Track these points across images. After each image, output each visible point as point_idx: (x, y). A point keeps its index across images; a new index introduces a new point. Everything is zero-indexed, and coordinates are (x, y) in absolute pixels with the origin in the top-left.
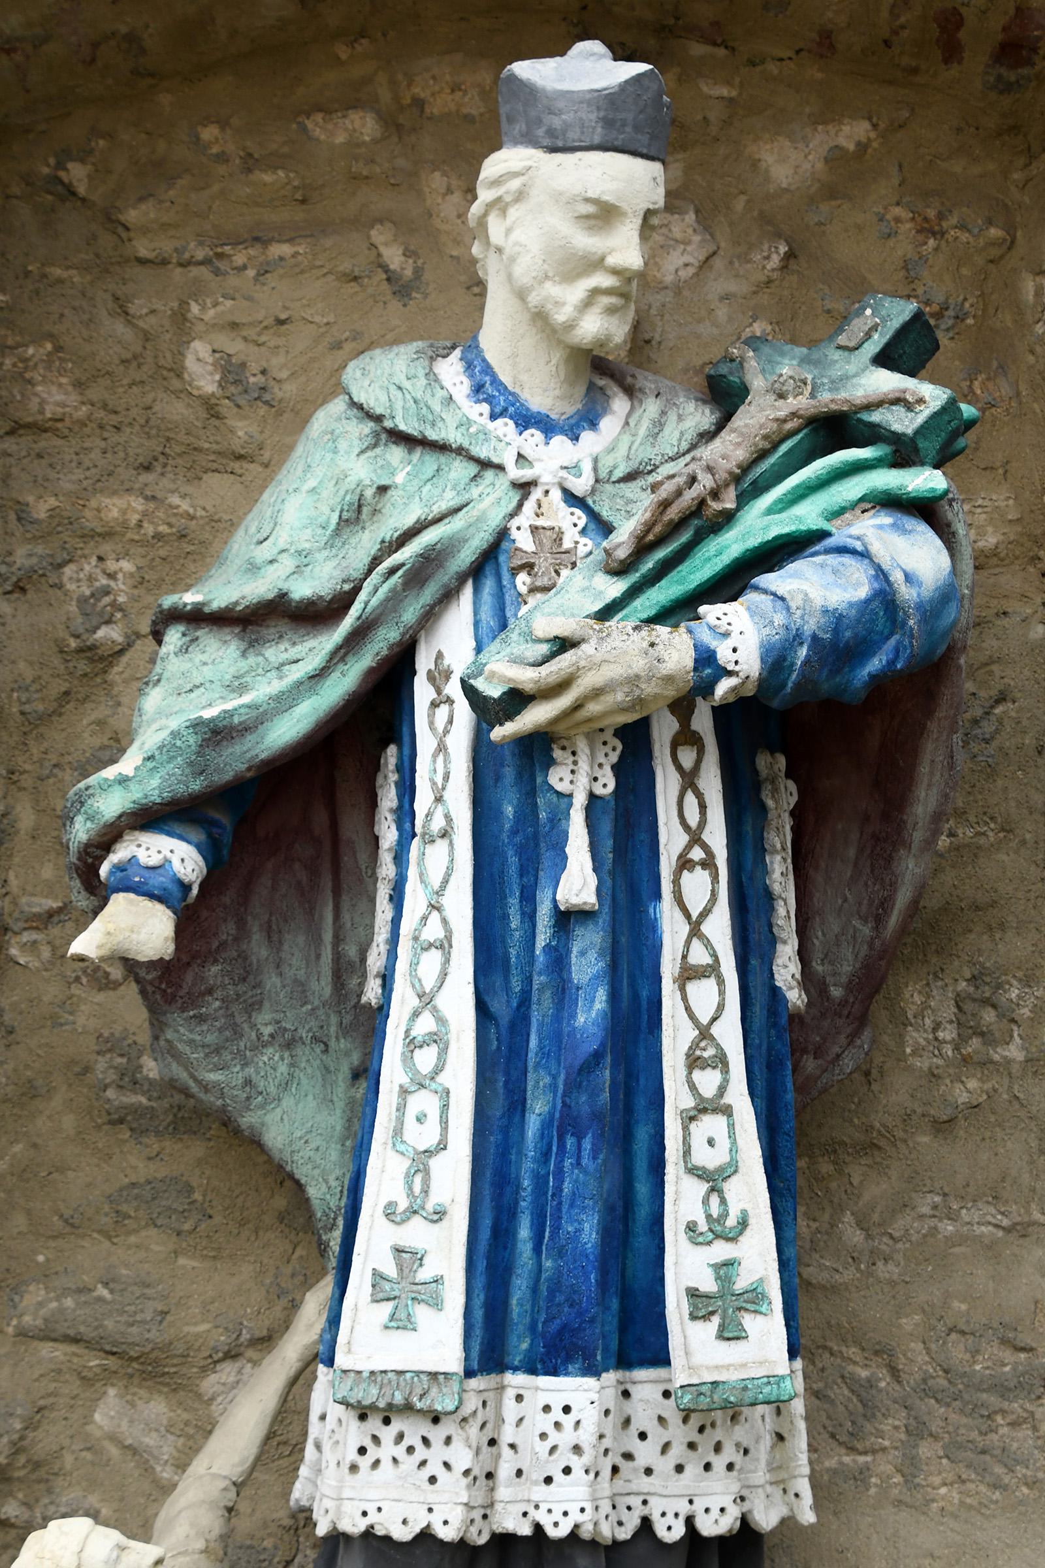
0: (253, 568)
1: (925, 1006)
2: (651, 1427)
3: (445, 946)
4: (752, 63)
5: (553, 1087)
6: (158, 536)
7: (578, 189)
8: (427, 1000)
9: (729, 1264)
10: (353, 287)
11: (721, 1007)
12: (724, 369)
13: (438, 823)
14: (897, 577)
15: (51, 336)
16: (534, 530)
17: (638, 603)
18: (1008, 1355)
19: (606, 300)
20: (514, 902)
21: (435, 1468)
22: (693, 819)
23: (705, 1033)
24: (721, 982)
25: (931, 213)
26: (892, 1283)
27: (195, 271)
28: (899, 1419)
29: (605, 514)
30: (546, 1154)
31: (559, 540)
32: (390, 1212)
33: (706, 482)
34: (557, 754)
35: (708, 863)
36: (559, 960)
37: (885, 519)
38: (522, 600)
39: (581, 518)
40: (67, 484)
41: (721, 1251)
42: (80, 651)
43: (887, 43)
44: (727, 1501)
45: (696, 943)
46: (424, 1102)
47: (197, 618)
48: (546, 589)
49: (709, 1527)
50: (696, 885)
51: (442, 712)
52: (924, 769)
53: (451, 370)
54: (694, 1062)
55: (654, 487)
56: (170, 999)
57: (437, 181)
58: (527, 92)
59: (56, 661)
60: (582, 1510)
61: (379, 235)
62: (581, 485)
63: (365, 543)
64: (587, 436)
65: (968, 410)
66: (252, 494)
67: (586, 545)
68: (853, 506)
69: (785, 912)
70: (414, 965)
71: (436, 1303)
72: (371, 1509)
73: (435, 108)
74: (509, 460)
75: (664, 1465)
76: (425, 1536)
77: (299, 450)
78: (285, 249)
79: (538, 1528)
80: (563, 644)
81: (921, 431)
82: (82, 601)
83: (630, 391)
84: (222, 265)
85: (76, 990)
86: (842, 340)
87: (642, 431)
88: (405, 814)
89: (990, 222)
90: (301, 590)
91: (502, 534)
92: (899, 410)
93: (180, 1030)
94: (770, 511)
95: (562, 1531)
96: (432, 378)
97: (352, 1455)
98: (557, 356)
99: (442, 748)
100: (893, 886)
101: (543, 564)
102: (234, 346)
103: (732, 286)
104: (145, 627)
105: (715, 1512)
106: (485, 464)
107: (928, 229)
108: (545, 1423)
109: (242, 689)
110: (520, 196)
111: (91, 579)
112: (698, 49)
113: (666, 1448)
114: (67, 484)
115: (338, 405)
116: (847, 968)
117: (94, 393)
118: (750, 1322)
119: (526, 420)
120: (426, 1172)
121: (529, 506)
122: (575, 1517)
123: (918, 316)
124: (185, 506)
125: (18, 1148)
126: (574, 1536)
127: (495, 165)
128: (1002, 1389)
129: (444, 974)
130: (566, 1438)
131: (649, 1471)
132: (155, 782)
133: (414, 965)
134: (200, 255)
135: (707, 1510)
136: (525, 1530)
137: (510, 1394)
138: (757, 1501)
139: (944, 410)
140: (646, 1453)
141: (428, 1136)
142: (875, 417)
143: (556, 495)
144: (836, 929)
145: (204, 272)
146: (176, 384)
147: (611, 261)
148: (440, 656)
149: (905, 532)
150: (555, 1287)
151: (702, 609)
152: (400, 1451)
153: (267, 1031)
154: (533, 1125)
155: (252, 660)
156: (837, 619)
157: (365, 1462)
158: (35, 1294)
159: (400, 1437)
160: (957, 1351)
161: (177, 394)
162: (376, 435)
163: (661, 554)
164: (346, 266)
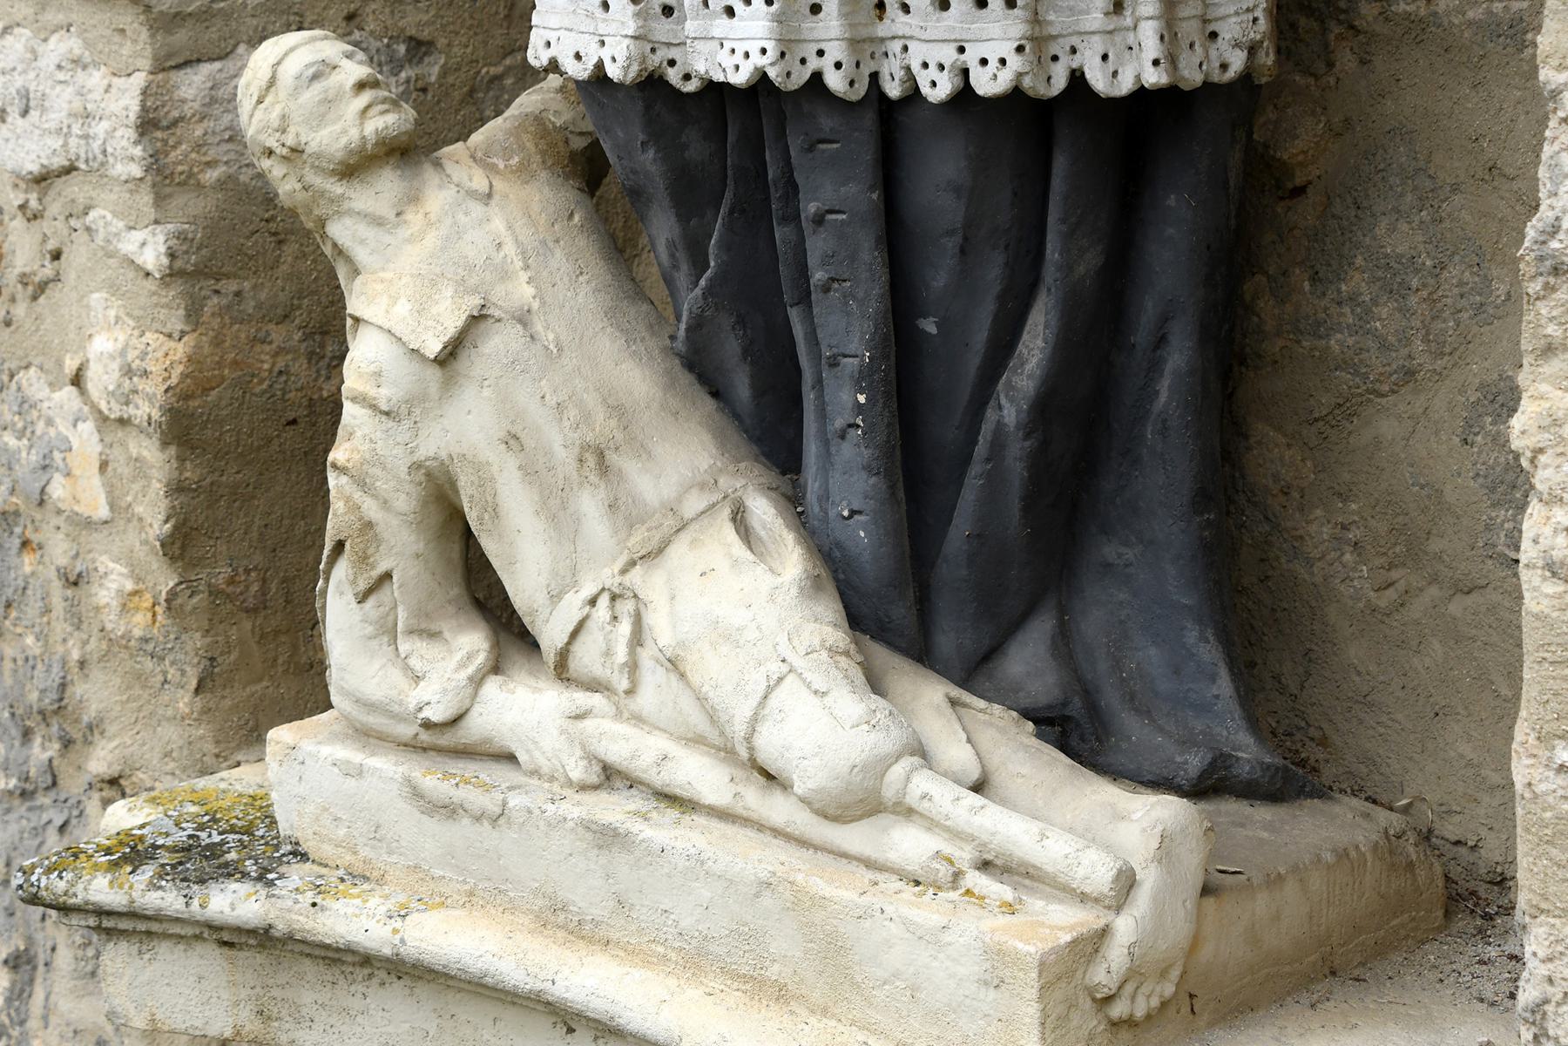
44: (1007, 49)
60: (764, 51)
76: (599, 77)
105: (993, 63)
122: (757, 60)
135: (984, 62)
138: (1088, 53)
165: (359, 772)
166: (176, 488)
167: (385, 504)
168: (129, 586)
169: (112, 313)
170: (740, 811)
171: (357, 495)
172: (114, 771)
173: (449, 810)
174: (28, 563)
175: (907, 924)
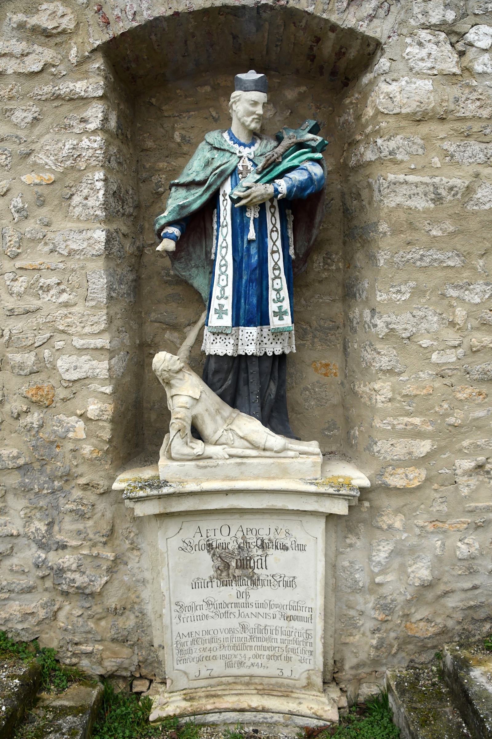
0: (188, 175)
1: (317, 259)
2: (266, 336)
3: (226, 247)
4: (283, 75)
5: (248, 274)
6: (170, 170)
7: (250, 99)
8: (223, 258)
9: (281, 306)
10: (206, 120)
11: (279, 258)
12: (279, 134)
13: (225, 223)
14: (313, 174)
15: (149, 132)
16: (242, 166)
17: (263, 180)
18: (331, 323)
19: (256, 120)
20: (239, 239)
21: (227, 343)
22: (274, 222)
23: (276, 263)
24: (279, 254)
25: (318, 105)
26: (310, 311)
27: (176, 118)
28: (311, 335)
29: (256, 162)
30: (246, 287)
31: (247, 167)
32: (217, 298)
33: (276, 156)
34: (247, 210)
35: (277, 231)
36: (248, 250)
37: (311, 163)
38: (240, 180)
39: (252, 164)
40: (152, 161)
41: (279, 304)
42: (155, 193)
43: (309, 72)
44: (280, 349)
45: (274, 246)
46: (223, 277)
47: (178, 185)
48: (245, 177)
49: (277, 353)
50: (274, 235)
51: (225, 202)
52: (318, 212)
53: (226, 135)
54: (274, 269)
55: (266, 157)
56: (175, 259)
57: (222, 99)
58: (240, 80)
59: (151, 195)
61: (211, 110)
62: (251, 157)
63: (210, 169)
64: (252, 147)
65: (326, 142)
66: (187, 161)
67: (252, 169)
68: (304, 160)
69: (291, 240)
70: (221, 251)
71: (227, 314)
72: (216, 350)
73: (222, 85)
74: (237, 152)
75: (269, 343)
76: (226, 355)
77: (197, 151)
78: (193, 113)
79: (246, 353)
80: (248, 188)
81: (317, 146)
82: (156, 183)
83: (261, 139)
84: (181, 117)
85: (157, 258)
86: (302, 128)
87: (263, 146)
88: (218, 222)
89: (329, 107)
90: (198, 179)
91: (236, 167)
92: (313, 142)
93: (177, 265)
94: (288, 161)
95: (251, 354)
96: (222, 137)
97: (212, 341)
98: (246, 132)
99: (225, 209)
100: (312, 235)
101: (244, 173)
102: (183, 132)
103: (280, 119)
104: (168, 188)
106: (233, 153)
107: (318, 108)
108: (247, 335)
109: (187, 199)
110: (239, 100)
111: (157, 179)
112: (273, 73)
113: (269, 340)
114: (152, 161)
115: (204, 142)
116: (303, 251)
117: (157, 143)
118: (284, 317)
119: (240, 144)
120: (224, 290)
121: (241, 161)
122: (253, 351)
123: (316, 124)
124: (175, 164)
125: (148, 288)
126: (252, 355)
127: (234, 94)
128: (330, 329)
129: (226, 253)
130: (251, 338)
131: (266, 344)
132: (171, 217)
133: (221, 251)
134: (177, 115)
136: (244, 354)
137: (241, 330)
139: (321, 142)
140: (265, 341)
141: (223, 283)
142: (308, 143)
143: (247, 159)
144: (301, 244)
145: (177, 118)
146: (172, 140)
147: (257, 112)
148: (224, 191)
149: (314, 165)
150: (249, 311)
151: (275, 181)
152: (221, 340)
153: (193, 265)
154: (244, 281)
155: (188, 193)
156: (301, 182)
157: (214, 342)
158: (153, 314)
159: (221, 338)
160: (322, 323)
161: (173, 142)
162: (211, 148)
163: (267, 170)
164: (205, 116)
165: (184, 465)
166: (112, 430)
167: (187, 423)
168: (93, 449)
169: (96, 402)
170: (260, 455)
171: (183, 422)
172: (88, 482)
173: (205, 467)
174: (57, 450)
175: (299, 463)
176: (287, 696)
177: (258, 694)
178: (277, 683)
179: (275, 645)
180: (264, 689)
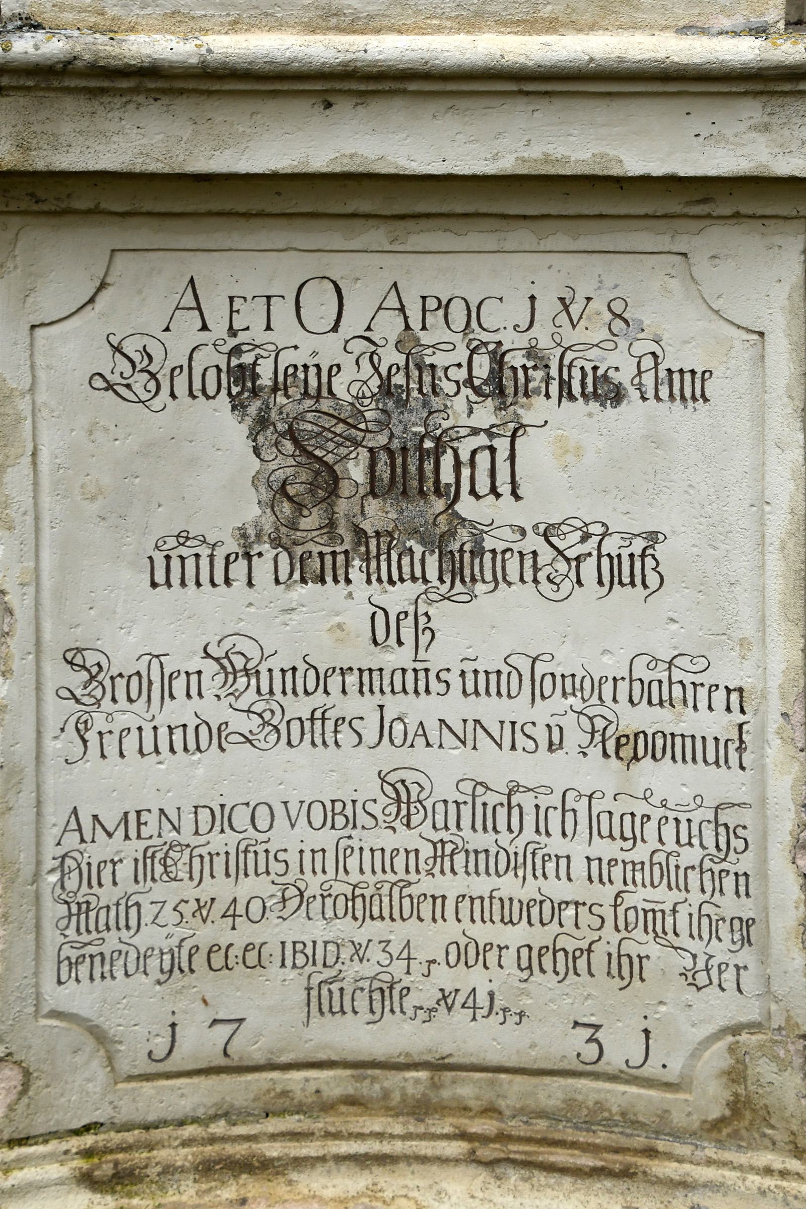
176: (626, 1173)
177: (472, 1159)
178: (571, 1104)
179: (558, 890)
180: (502, 1137)
